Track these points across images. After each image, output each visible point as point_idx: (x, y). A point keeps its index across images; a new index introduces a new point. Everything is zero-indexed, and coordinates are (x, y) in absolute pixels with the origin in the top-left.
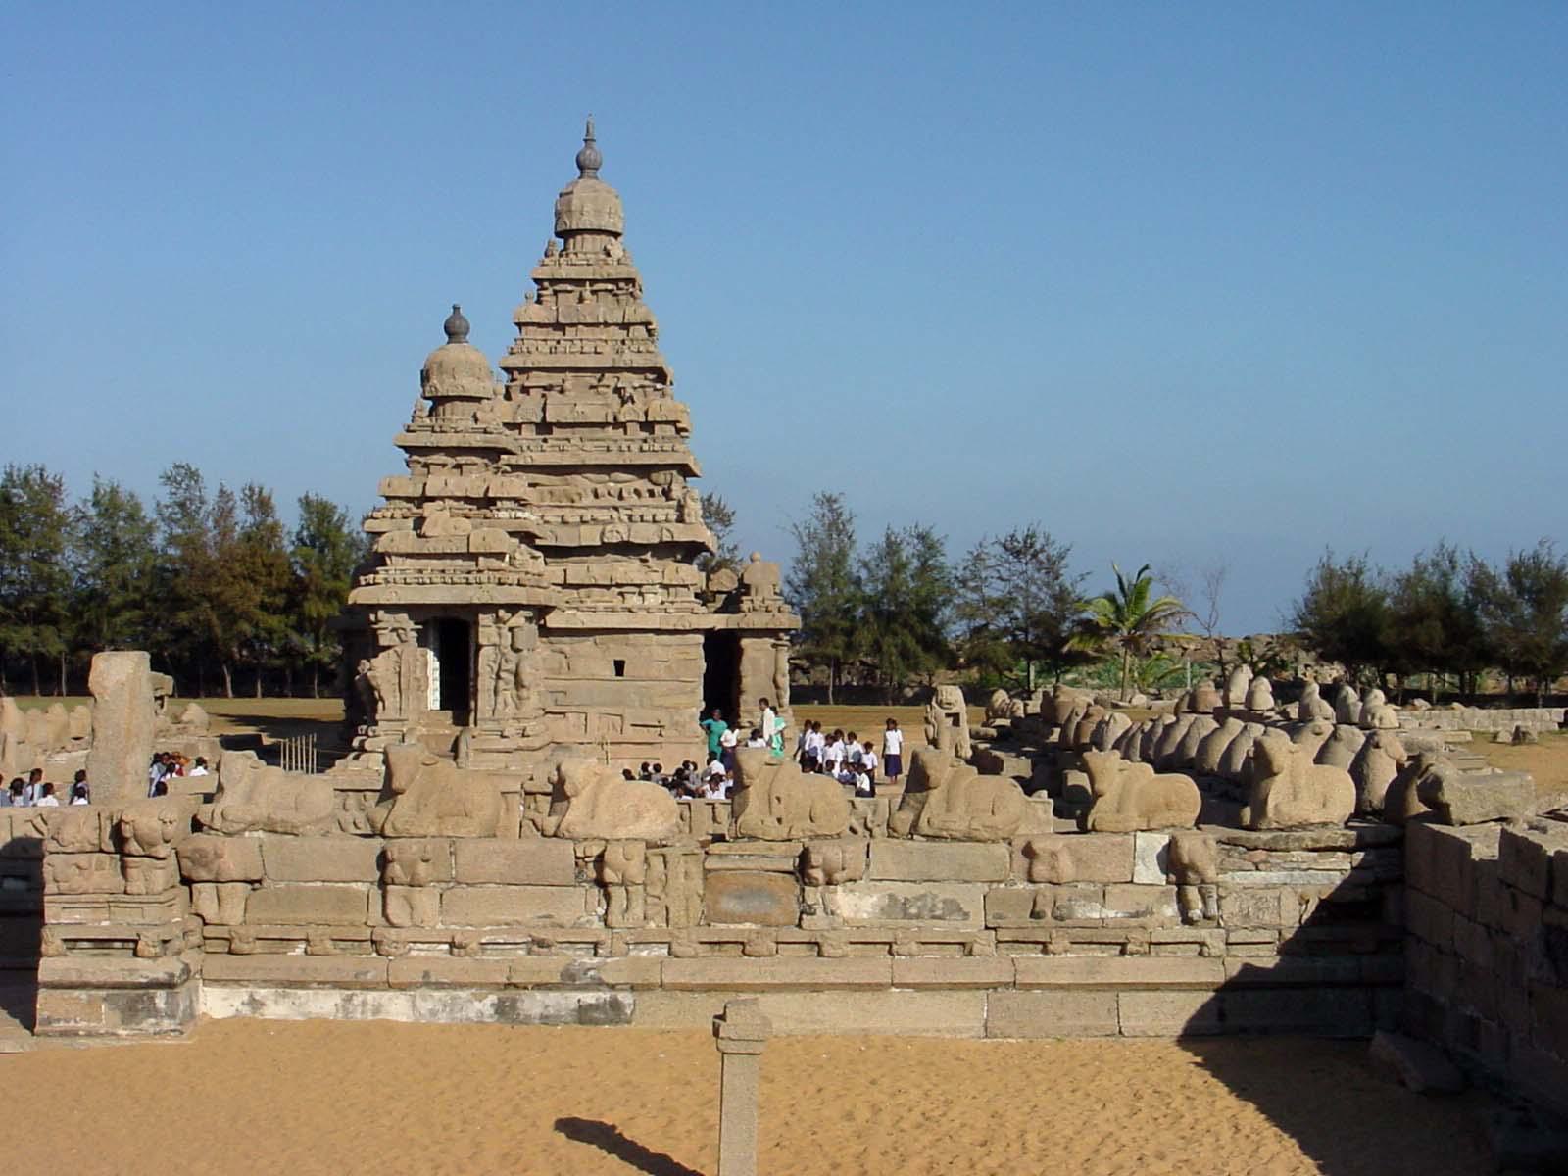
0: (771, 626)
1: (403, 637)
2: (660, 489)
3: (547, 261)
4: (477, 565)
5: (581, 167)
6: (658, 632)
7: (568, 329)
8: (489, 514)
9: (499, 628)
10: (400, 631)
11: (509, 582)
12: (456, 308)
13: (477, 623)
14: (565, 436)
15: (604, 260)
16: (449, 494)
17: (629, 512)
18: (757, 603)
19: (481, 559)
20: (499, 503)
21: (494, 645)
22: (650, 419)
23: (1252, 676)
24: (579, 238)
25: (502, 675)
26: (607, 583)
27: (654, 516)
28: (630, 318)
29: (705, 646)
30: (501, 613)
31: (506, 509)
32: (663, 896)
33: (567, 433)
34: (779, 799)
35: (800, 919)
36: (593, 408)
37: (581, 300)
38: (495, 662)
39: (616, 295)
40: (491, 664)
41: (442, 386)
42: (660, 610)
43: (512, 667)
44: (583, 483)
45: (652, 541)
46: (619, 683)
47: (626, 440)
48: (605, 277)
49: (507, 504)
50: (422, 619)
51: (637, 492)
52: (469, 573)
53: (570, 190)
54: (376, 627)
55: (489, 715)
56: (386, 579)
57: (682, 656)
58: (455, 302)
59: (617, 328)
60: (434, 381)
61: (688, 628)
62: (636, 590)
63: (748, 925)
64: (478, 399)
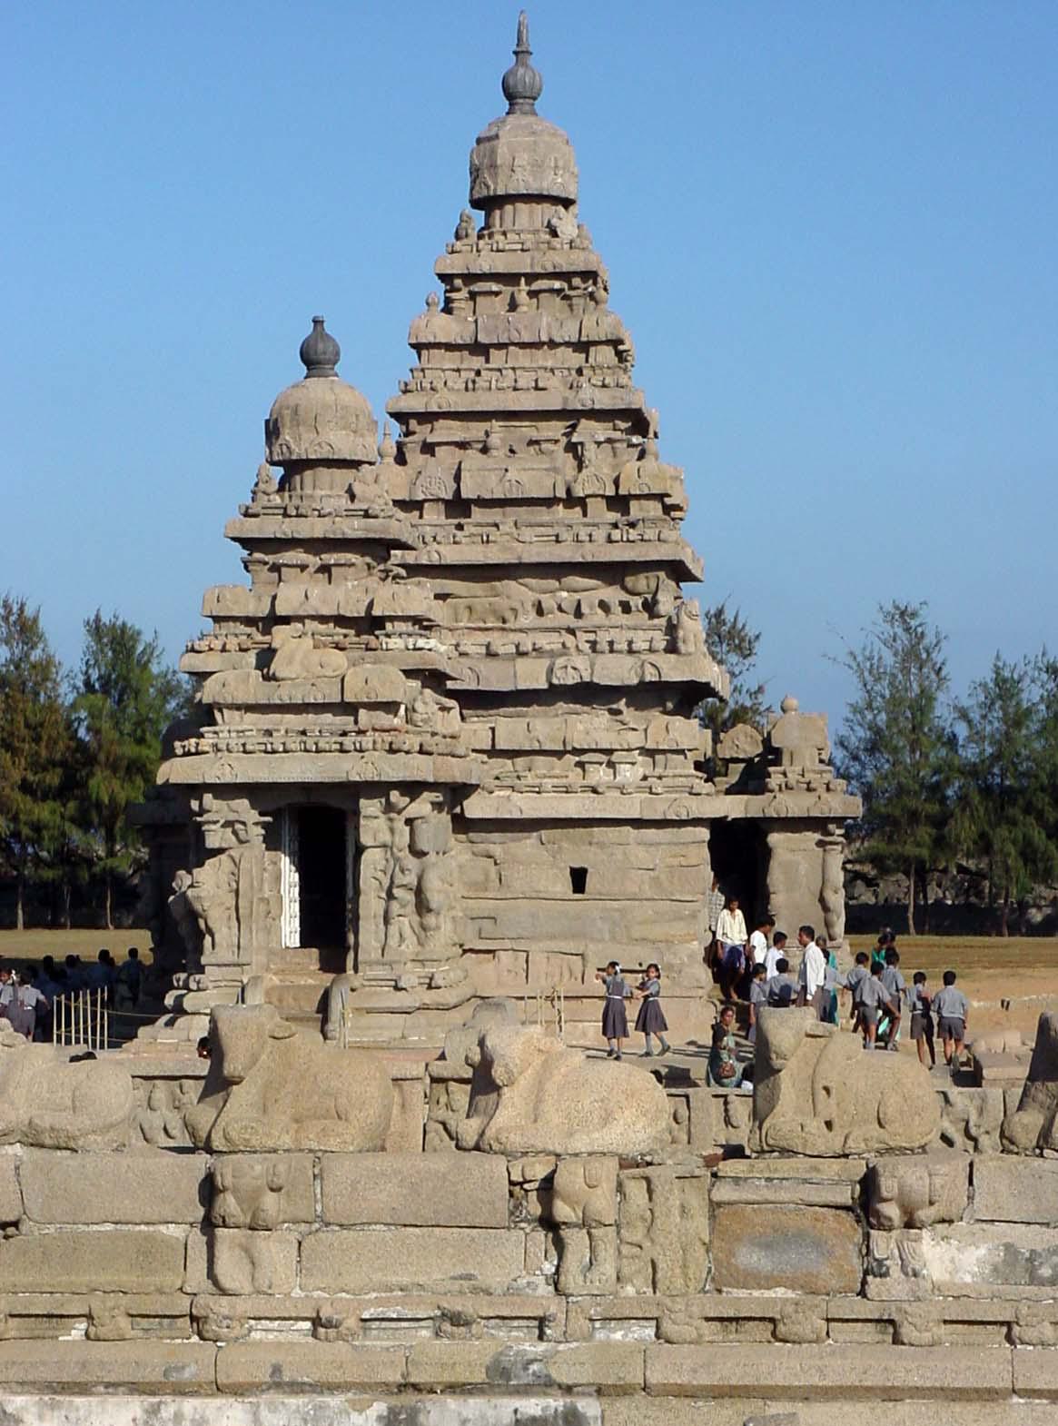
0: (815, 813)
1: (242, 834)
3: (458, 245)
4: (356, 722)
5: (510, 95)
6: (638, 823)
8: (373, 642)
9: (391, 820)
10: (238, 826)
11: (406, 747)
13: (357, 813)
15: (548, 243)
17: (592, 637)
18: (793, 778)
19: (362, 712)
20: (389, 626)
21: (384, 846)
22: (622, 492)
24: (509, 208)
25: (396, 891)
27: (630, 643)
28: (590, 333)
29: (712, 845)
30: (395, 796)
32: (647, 1244)
33: (494, 515)
34: (827, 1089)
35: (864, 1283)
36: (531, 476)
37: (513, 306)
39: (566, 298)
40: (380, 875)
41: (300, 444)
42: (639, 789)
43: (411, 879)
44: (519, 592)
45: (627, 682)
46: (579, 905)
48: (551, 269)
50: (272, 807)
51: (604, 606)
52: (344, 734)
53: (493, 133)
54: (199, 819)
55: (376, 955)
56: (215, 745)
57: (675, 862)
58: (319, 314)
60: (286, 436)
61: (684, 817)
62: (604, 758)
63: (780, 1292)
64: (354, 464)
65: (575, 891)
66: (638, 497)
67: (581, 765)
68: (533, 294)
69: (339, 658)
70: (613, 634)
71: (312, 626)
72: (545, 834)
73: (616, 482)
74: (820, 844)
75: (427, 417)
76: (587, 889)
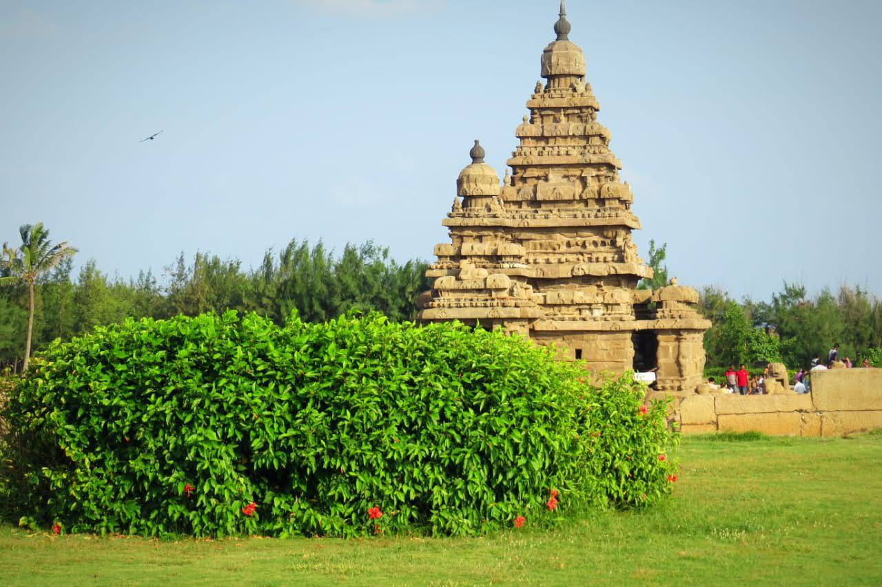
0: (675, 327)
6: (602, 332)
17: (589, 256)
22: (602, 197)
27: (605, 258)
33: (550, 207)
41: (471, 189)
44: (560, 238)
47: (587, 210)
49: (508, 259)
52: (486, 300)
57: (615, 347)
60: (465, 186)
62: (588, 307)
66: (609, 199)
67: (580, 310)
68: (566, 115)
69: (484, 272)
71: (475, 259)
73: (599, 194)
75: (525, 167)
76: (582, 357)
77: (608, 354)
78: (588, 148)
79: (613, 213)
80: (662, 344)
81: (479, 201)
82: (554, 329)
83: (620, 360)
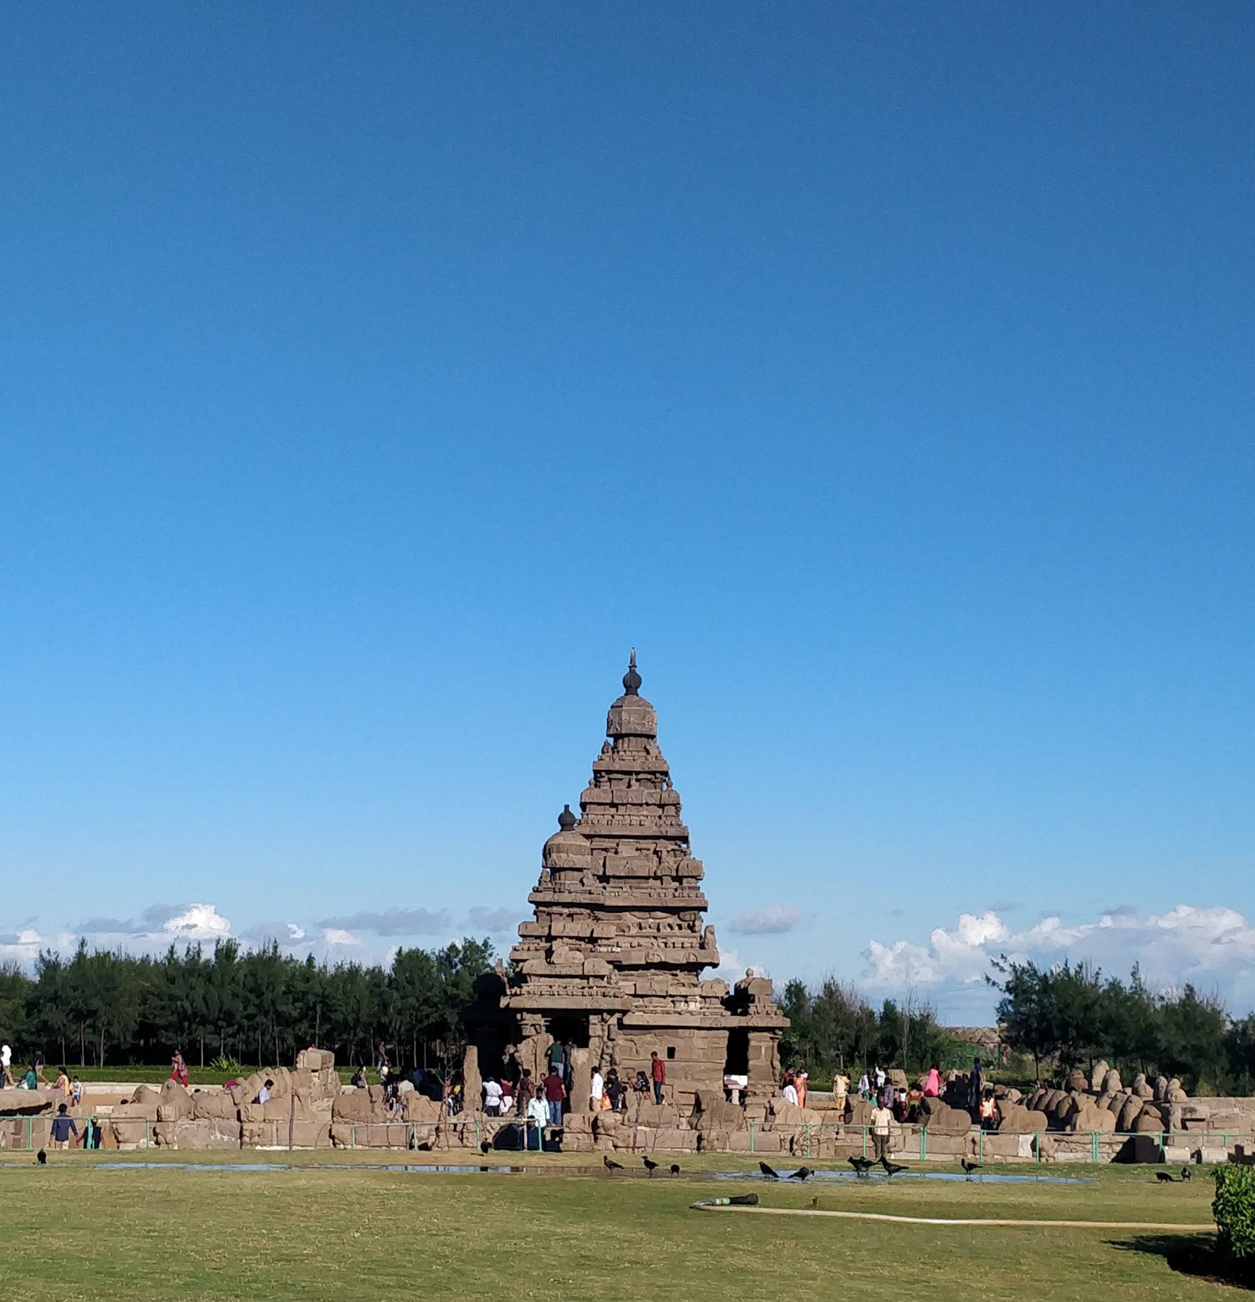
0: (770, 1025)
1: (539, 1031)
2: (686, 924)
7: (619, 806)
9: (602, 1025)
12: (567, 807)
13: (588, 1021)
14: (620, 885)
16: (566, 934)
17: (664, 940)
19: (591, 979)
20: (599, 941)
21: (599, 1036)
22: (680, 874)
23: (1108, 1068)
24: (626, 739)
25: (605, 1056)
26: (665, 994)
27: (683, 944)
29: (730, 1039)
30: (605, 1015)
31: (605, 945)
37: (629, 786)
38: (599, 1048)
39: (653, 782)
40: (597, 1049)
41: (560, 859)
42: (700, 1013)
48: (647, 770)
51: (670, 926)
52: (583, 988)
59: (656, 807)
60: (554, 855)
62: (683, 999)
64: (580, 870)
65: (669, 1057)
67: (673, 1002)
70: (674, 940)
71: (565, 940)
72: (656, 1031)
73: (677, 870)
74: (771, 1038)
76: (676, 1056)
77: (705, 1055)
78: (664, 819)
79: (693, 894)
80: (752, 1043)
81: (569, 873)
82: (646, 1024)
83: (719, 1061)
